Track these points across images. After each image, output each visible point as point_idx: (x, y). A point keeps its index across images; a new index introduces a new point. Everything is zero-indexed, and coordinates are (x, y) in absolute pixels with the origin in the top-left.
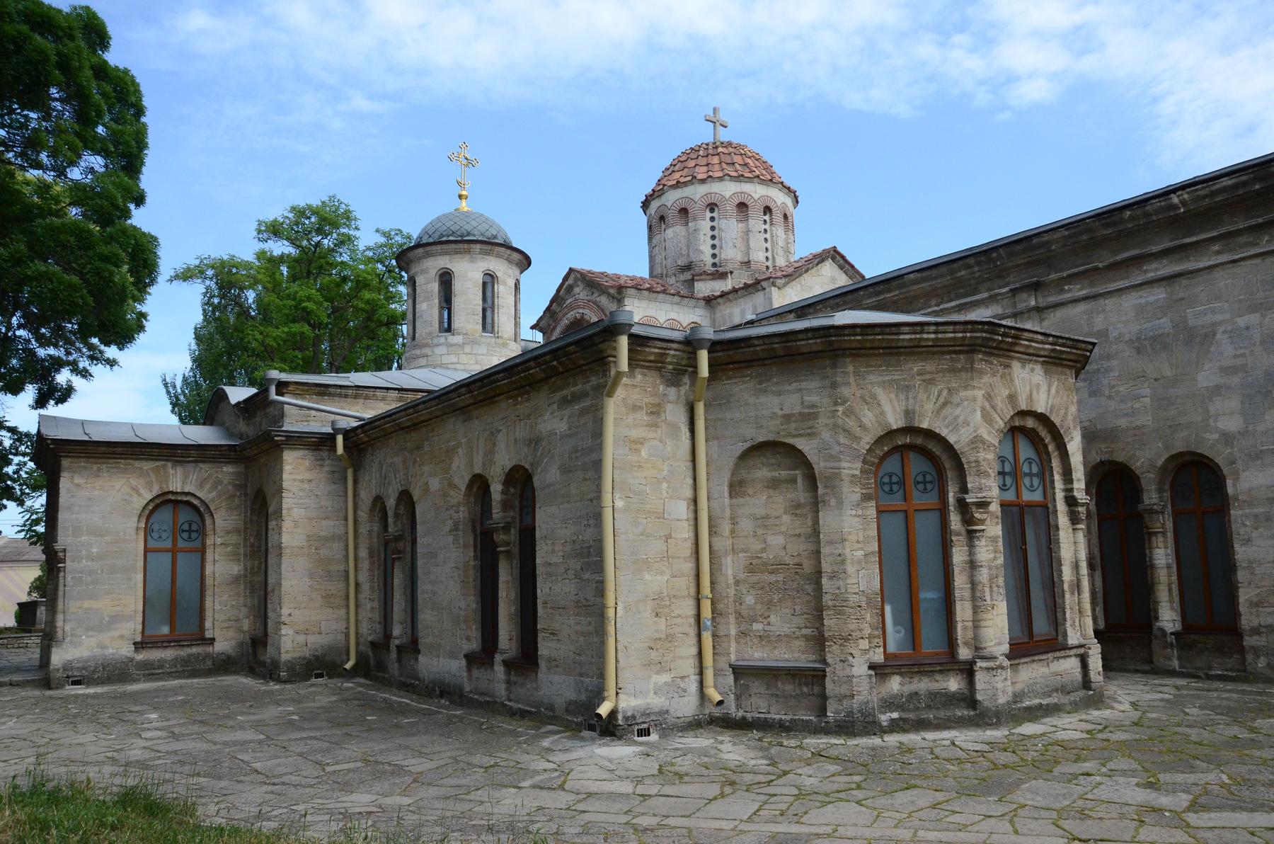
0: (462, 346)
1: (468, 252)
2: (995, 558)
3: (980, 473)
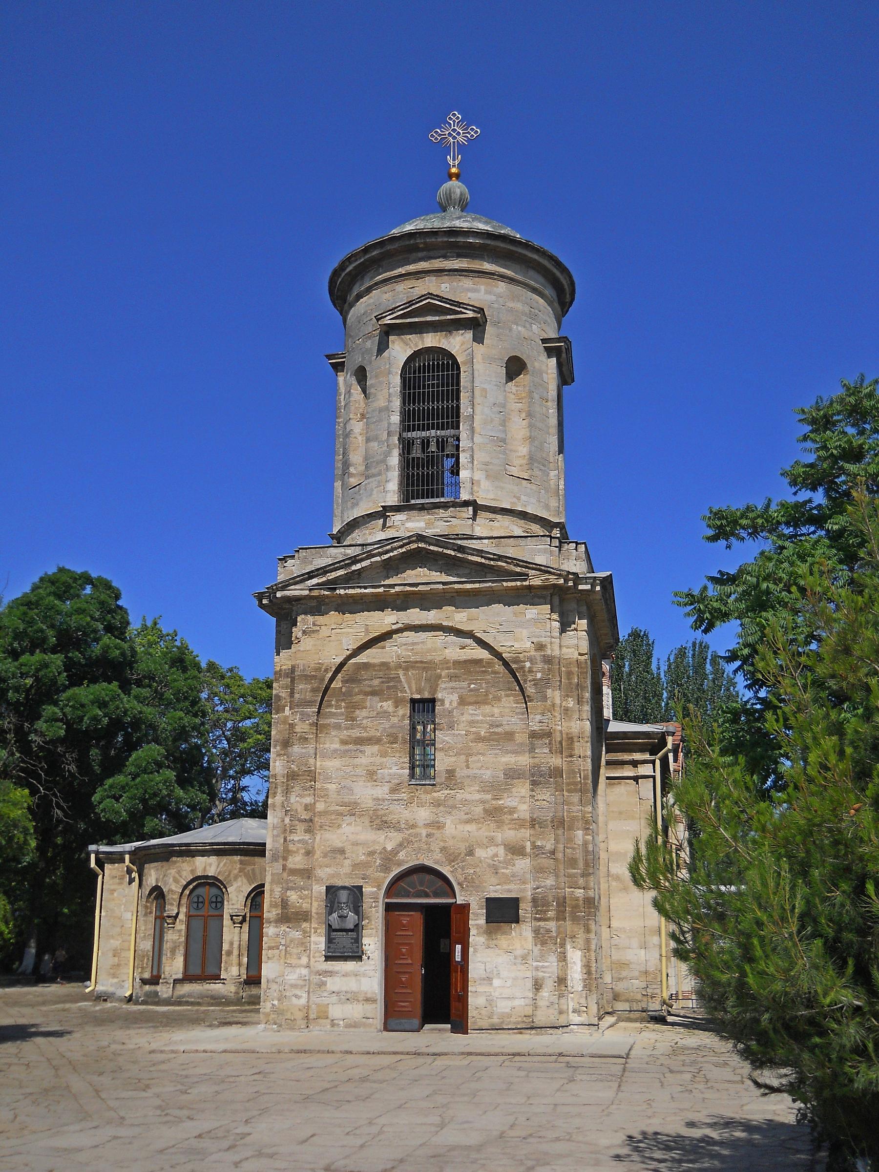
3: (172, 904)
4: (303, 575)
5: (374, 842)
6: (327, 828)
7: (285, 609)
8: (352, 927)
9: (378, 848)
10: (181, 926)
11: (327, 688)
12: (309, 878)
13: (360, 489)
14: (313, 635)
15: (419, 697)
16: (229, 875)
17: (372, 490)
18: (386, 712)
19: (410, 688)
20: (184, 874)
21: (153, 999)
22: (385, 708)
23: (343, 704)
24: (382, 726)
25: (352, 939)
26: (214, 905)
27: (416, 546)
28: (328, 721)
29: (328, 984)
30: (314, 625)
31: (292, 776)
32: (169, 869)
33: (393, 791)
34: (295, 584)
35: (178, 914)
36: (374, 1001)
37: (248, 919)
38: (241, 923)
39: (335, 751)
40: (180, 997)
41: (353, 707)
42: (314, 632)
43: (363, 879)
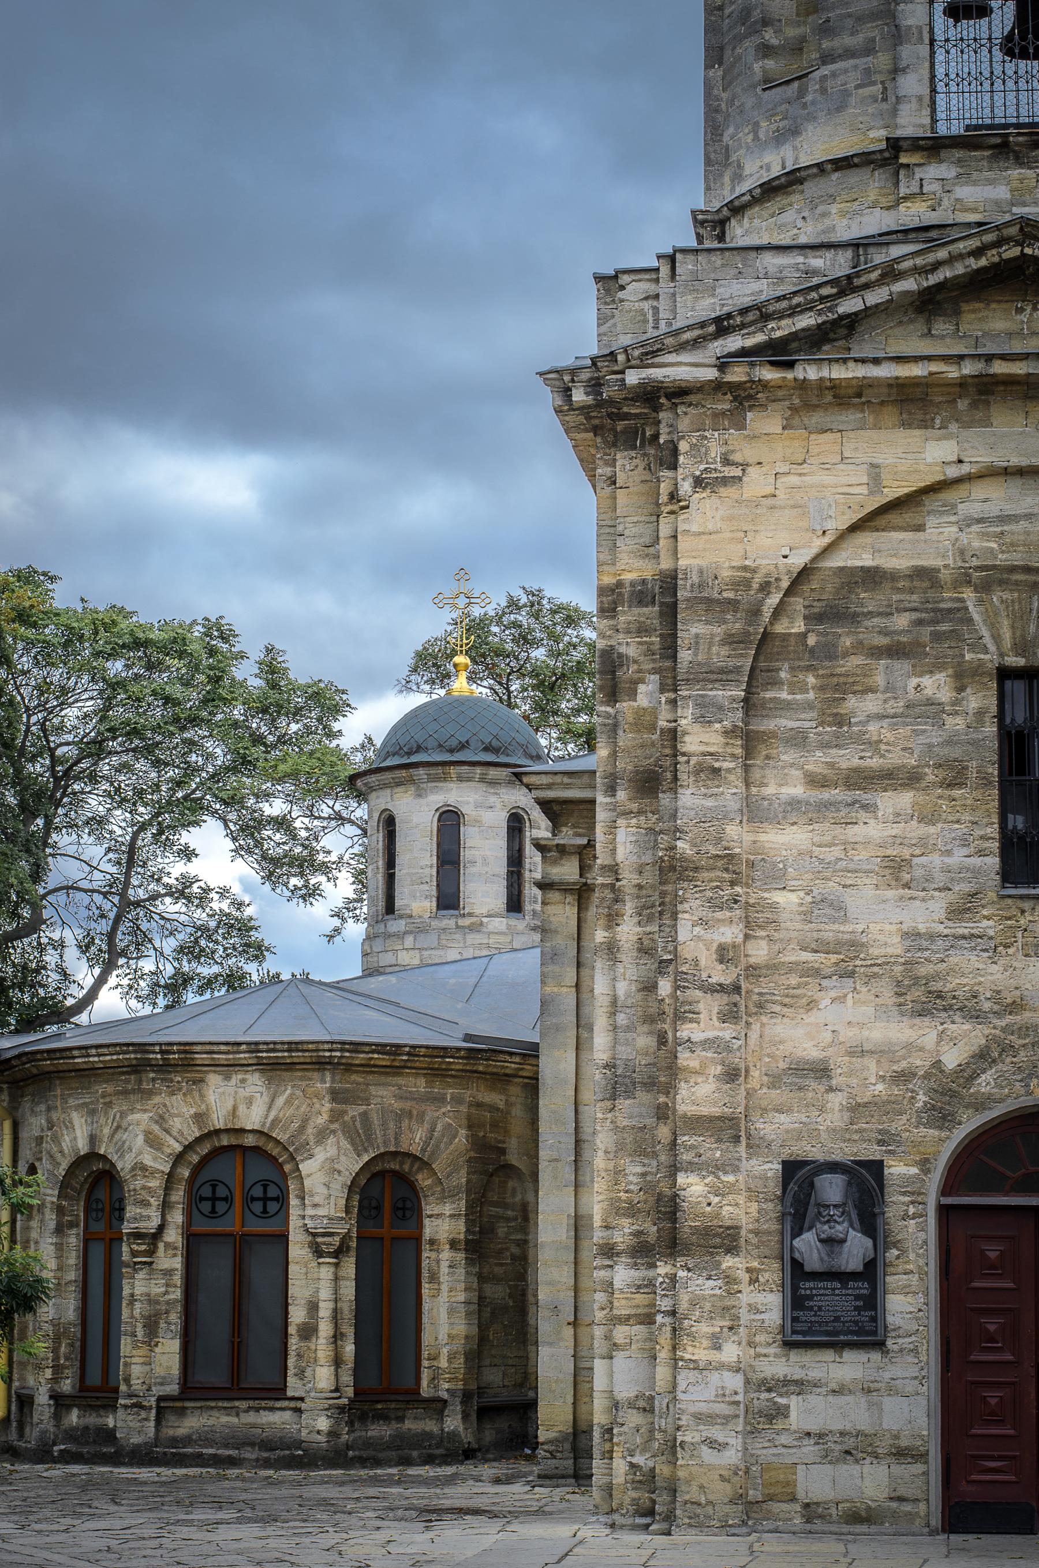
0: (401, 936)
1: (411, 781)
2: (166, 1293)
4: (702, 325)
5: (909, 1046)
6: (777, 1008)
7: (627, 416)
8: (861, 1268)
9: (920, 1062)
10: (171, 1260)
11: (765, 634)
12: (736, 1139)
13: (802, 93)
14: (723, 491)
15: (1021, 662)
16: (302, 1128)
17: (846, 94)
18: (930, 702)
19: (997, 638)
20: (176, 1124)
21: (103, 1448)
22: (929, 692)
23: (811, 680)
24: (922, 740)
25: (857, 1297)
26: (257, 1207)
27: (1016, 251)
28: (770, 725)
29: (793, 1414)
30: (727, 462)
31: (671, 871)
32: (132, 1111)
33: (957, 912)
34: (681, 347)
35: (161, 1228)
36: (922, 1457)
37: (354, 1244)
38: (339, 1253)
39: (794, 804)
40: (175, 1441)
41: (837, 689)
42: (725, 481)
43: (881, 1142)
